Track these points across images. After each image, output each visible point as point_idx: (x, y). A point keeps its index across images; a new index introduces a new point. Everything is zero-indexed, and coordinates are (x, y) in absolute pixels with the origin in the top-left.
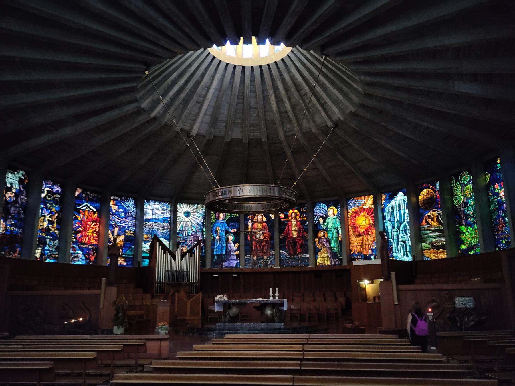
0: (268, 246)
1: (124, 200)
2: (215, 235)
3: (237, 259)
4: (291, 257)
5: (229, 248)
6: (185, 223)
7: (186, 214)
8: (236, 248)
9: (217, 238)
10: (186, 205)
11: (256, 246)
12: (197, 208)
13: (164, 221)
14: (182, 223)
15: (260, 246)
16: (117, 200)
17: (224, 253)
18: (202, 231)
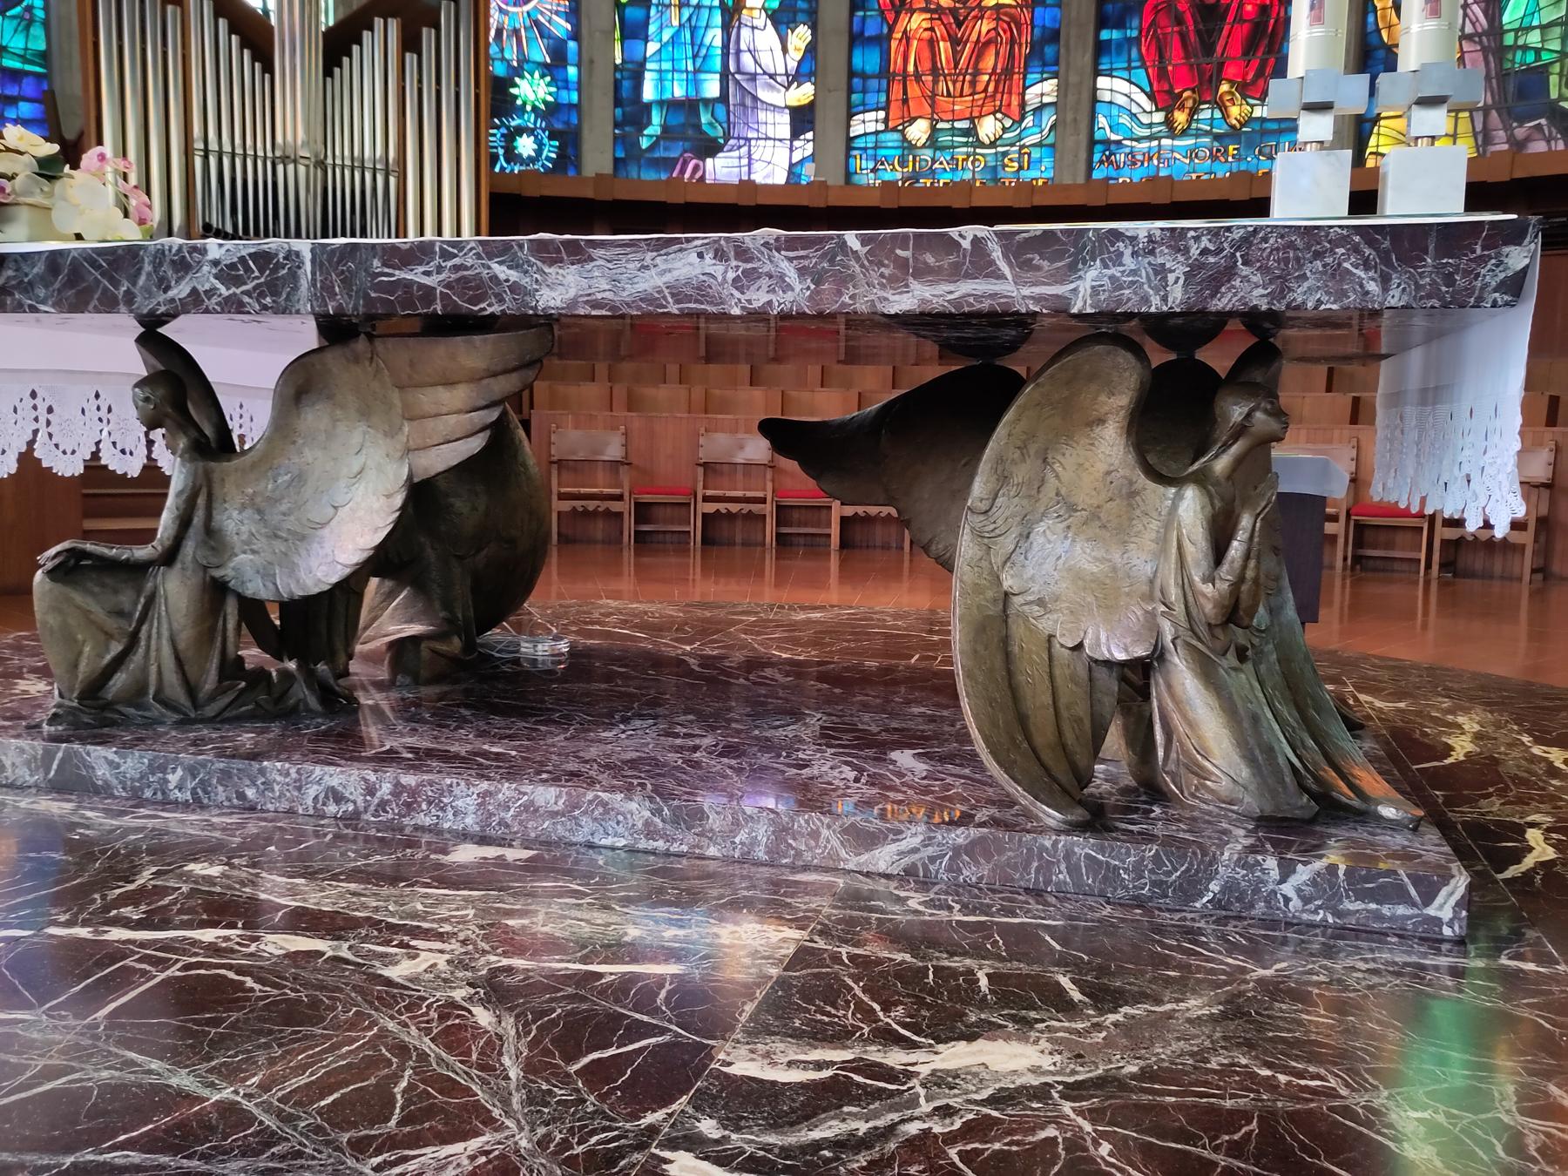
0: (1012, 41)
3: (795, 134)
4: (1169, 122)
5: (747, 61)
8: (795, 55)
11: (932, 44)
15: (956, 42)
17: (711, 88)
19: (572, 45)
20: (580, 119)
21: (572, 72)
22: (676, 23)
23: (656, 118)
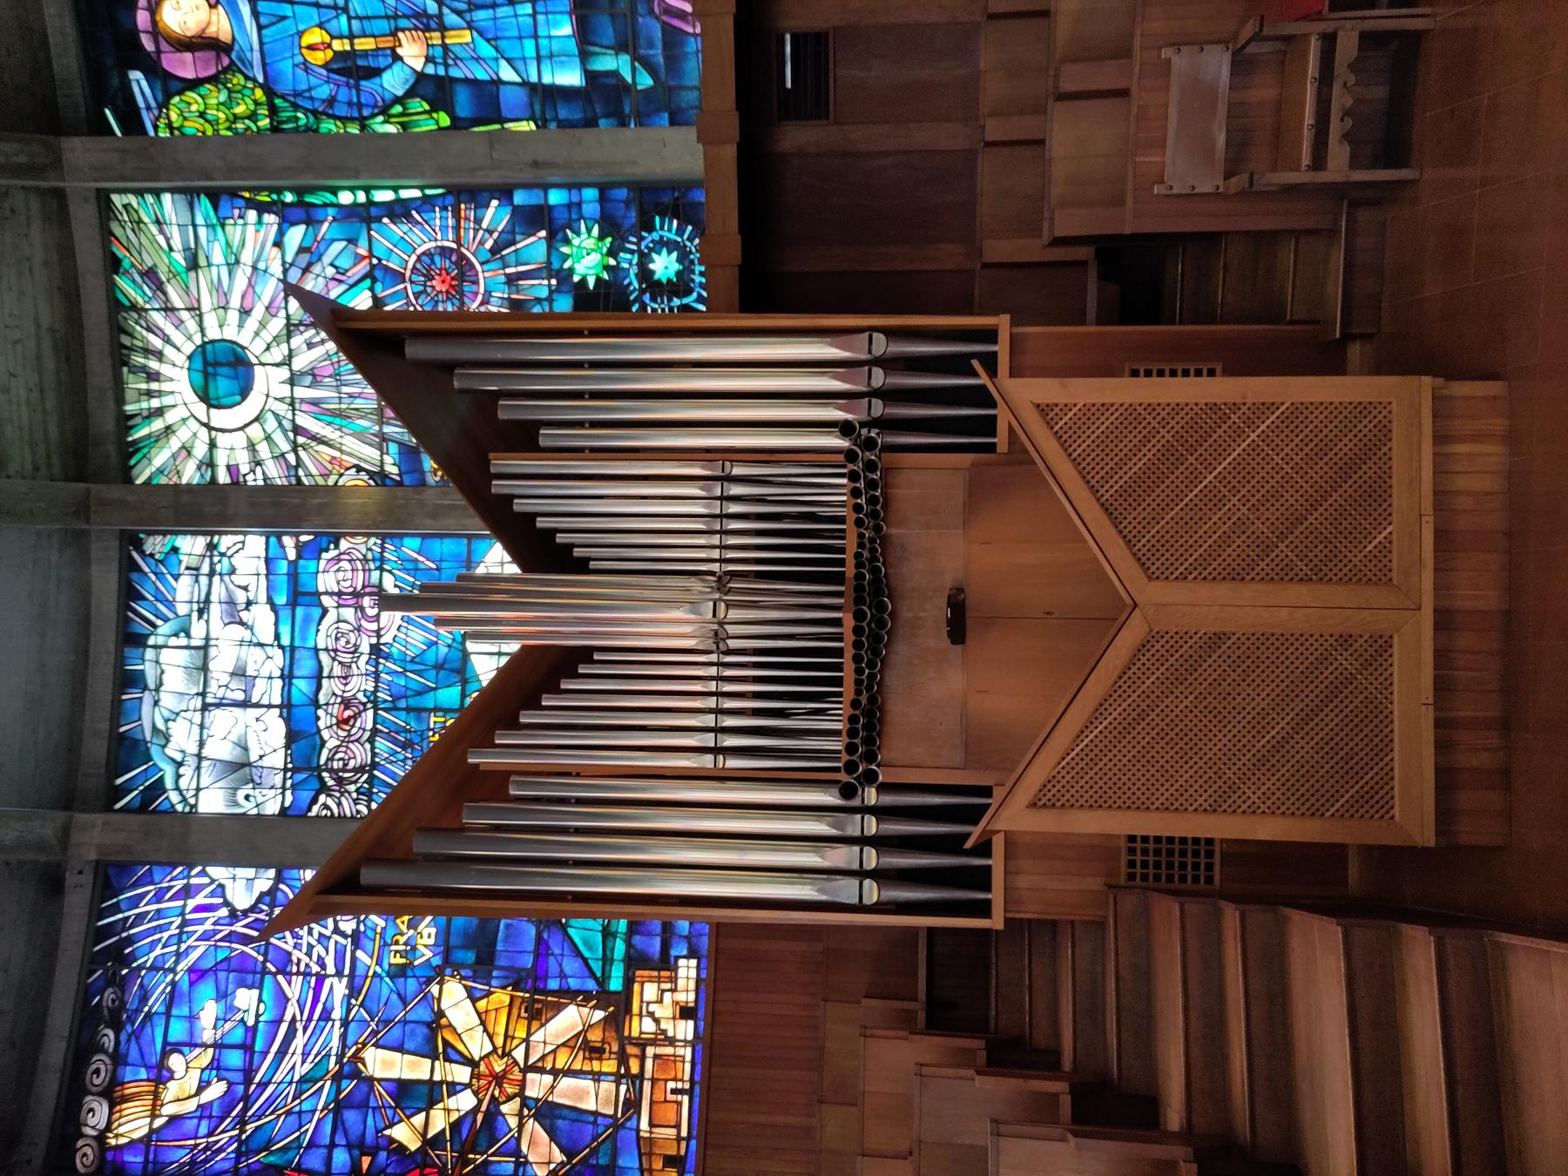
1: (122, 985)
2: (394, 81)
6: (300, 392)
7: (222, 385)
9: (413, 52)
10: (135, 384)
12: (150, 275)
13: (301, 596)
14: (304, 421)
16: (118, 1059)
18: (365, 215)
19: (520, 198)
20: (619, 185)
21: (556, 197)
22: (466, 37)
23: (606, 62)
